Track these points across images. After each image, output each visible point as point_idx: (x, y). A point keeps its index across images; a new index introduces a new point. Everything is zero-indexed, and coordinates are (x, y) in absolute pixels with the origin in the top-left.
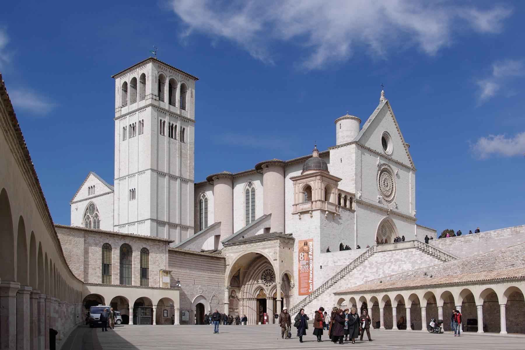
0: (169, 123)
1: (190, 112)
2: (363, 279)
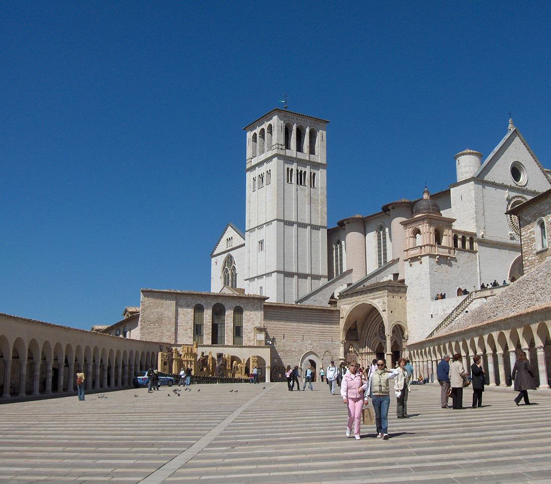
0: (297, 171)
1: (320, 155)
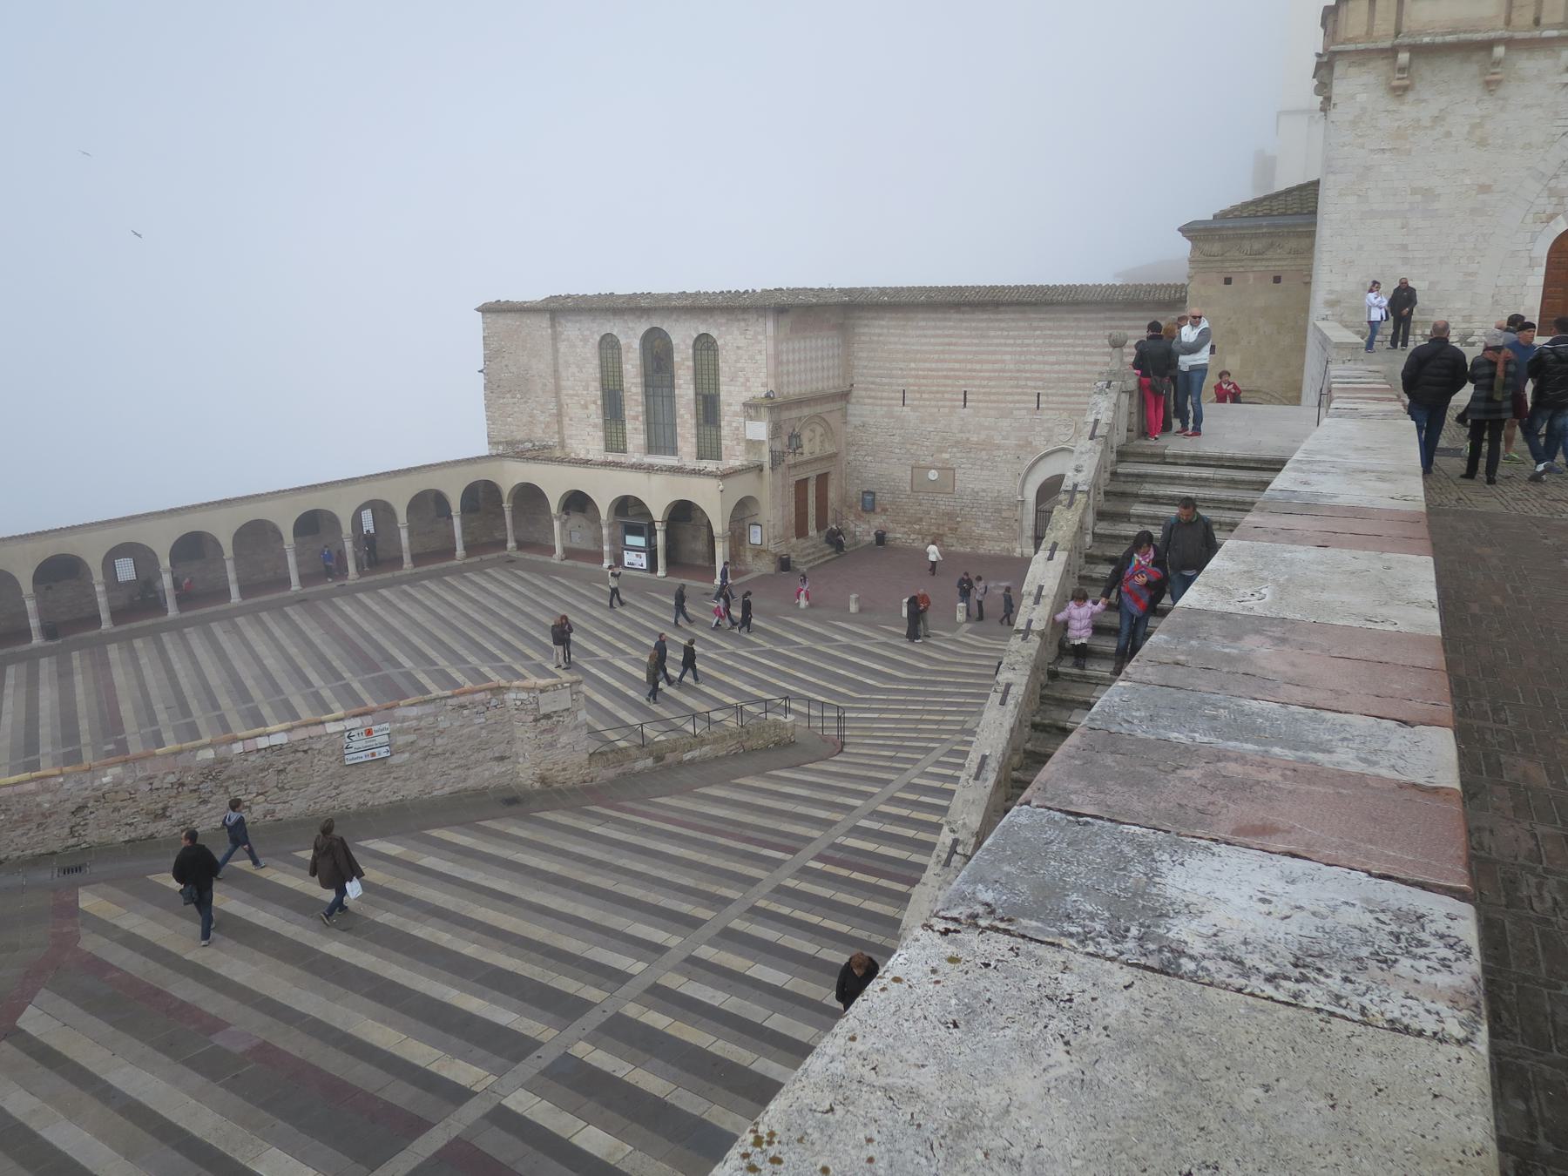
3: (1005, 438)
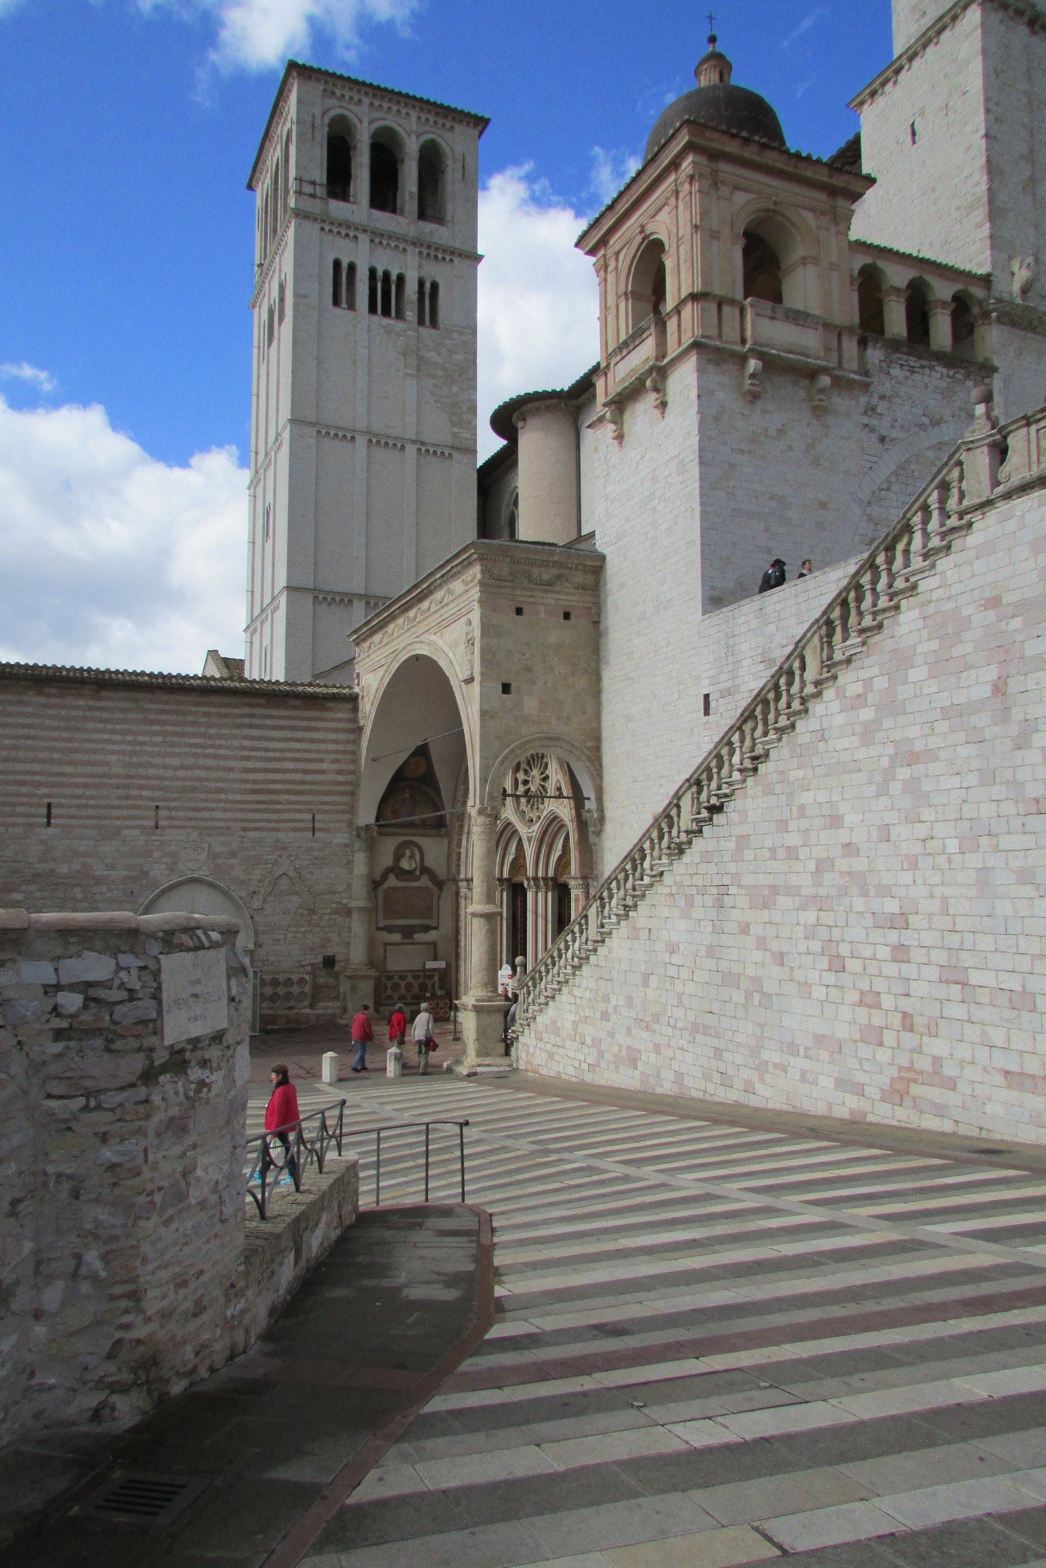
2: (889, 775)
3: (111, 867)
